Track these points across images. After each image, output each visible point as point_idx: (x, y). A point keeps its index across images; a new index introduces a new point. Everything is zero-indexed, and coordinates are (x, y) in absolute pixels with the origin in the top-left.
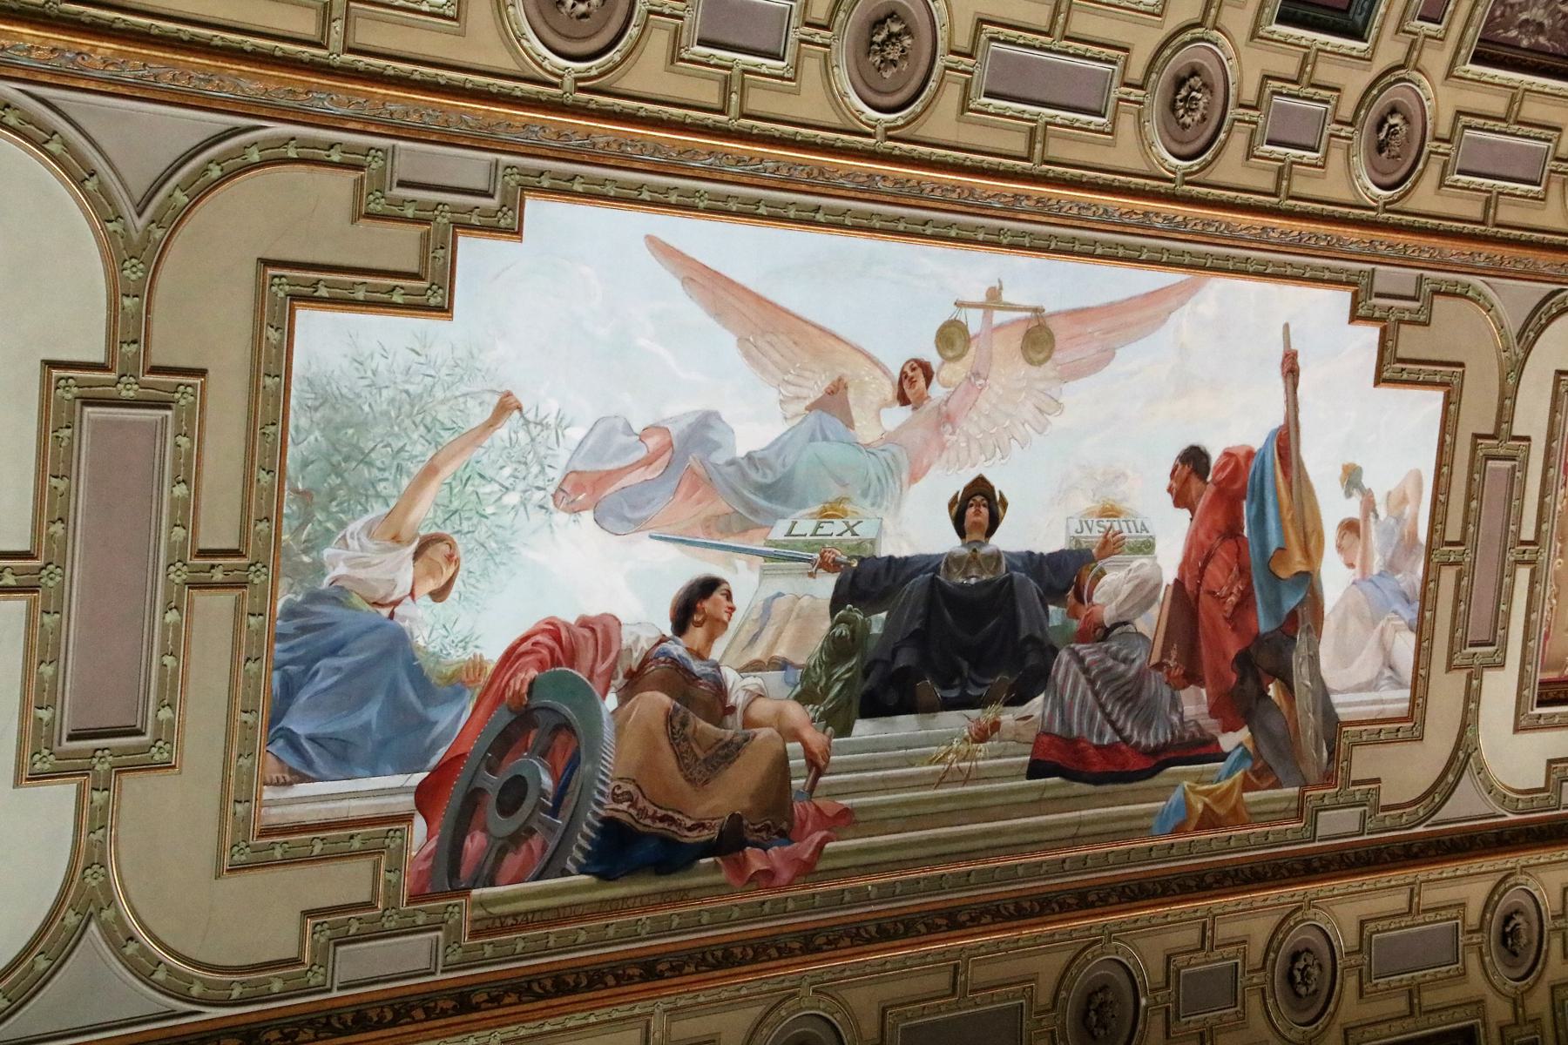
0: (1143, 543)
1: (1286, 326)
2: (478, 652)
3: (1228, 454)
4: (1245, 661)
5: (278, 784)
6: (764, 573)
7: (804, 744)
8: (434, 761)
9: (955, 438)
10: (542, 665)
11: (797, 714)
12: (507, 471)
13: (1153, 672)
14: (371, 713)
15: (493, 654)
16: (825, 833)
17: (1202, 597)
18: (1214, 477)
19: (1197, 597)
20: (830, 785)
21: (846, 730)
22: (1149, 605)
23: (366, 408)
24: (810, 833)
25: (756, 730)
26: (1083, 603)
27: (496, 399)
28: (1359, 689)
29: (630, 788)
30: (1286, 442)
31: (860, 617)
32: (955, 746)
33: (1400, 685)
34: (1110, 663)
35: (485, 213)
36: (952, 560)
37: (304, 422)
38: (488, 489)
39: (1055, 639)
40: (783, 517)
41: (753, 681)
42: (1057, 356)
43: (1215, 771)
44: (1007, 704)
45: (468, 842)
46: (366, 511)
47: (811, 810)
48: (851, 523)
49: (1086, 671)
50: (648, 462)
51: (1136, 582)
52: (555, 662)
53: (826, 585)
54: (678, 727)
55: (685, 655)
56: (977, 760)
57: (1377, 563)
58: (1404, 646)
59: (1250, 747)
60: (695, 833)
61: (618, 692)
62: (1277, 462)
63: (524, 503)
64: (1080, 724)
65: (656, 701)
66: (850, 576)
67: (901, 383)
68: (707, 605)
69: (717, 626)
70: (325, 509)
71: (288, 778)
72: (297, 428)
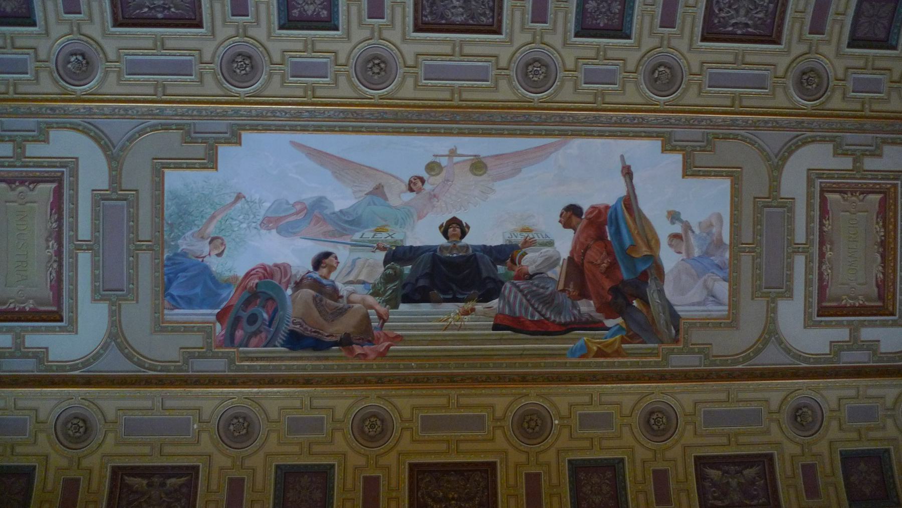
0: (547, 242)
1: (622, 157)
2: (236, 273)
3: (594, 208)
4: (615, 290)
5: (169, 309)
6: (351, 251)
7: (376, 310)
8: (222, 306)
9: (439, 203)
10: (260, 278)
11: (371, 300)
12: (241, 217)
13: (560, 293)
14: (198, 290)
15: (241, 274)
16: (389, 343)
17: (586, 265)
18: (586, 218)
19: (583, 264)
20: (390, 326)
21: (396, 307)
22: (555, 266)
23: (190, 199)
24: (381, 343)
25: (354, 305)
26: (516, 264)
27: (235, 195)
28: (693, 304)
29: (300, 321)
30: (629, 202)
31: (398, 267)
32: (452, 316)
33: (720, 303)
34: (535, 288)
35: (226, 138)
36: (442, 248)
37: (169, 203)
38: (234, 223)
39: (502, 279)
40: (357, 231)
41: (350, 288)
42: (489, 172)
43: (603, 334)
44: (479, 301)
45: (237, 332)
46: (191, 229)
47: (382, 334)
48: (391, 234)
49: (521, 291)
50: (297, 213)
51: (547, 257)
52: (265, 277)
53: (381, 255)
54: (318, 301)
55: (319, 277)
56: (464, 322)
57: (696, 252)
58: (722, 289)
59: (624, 326)
60: (330, 338)
61: (292, 288)
62: (625, 210)
63: (249, 227)
64: (520, 311)
65: (307, 293)
66: (392, 252)
67: (409, 184)
68: (327, 261)
69: (332, 269)
70: (178, 229)
71: (172, 308)
72: (167, 205)
